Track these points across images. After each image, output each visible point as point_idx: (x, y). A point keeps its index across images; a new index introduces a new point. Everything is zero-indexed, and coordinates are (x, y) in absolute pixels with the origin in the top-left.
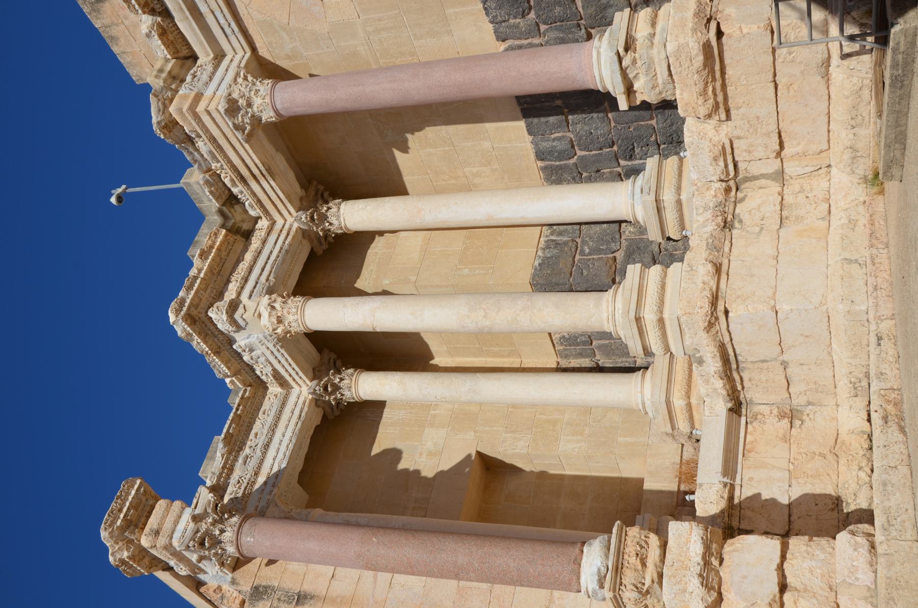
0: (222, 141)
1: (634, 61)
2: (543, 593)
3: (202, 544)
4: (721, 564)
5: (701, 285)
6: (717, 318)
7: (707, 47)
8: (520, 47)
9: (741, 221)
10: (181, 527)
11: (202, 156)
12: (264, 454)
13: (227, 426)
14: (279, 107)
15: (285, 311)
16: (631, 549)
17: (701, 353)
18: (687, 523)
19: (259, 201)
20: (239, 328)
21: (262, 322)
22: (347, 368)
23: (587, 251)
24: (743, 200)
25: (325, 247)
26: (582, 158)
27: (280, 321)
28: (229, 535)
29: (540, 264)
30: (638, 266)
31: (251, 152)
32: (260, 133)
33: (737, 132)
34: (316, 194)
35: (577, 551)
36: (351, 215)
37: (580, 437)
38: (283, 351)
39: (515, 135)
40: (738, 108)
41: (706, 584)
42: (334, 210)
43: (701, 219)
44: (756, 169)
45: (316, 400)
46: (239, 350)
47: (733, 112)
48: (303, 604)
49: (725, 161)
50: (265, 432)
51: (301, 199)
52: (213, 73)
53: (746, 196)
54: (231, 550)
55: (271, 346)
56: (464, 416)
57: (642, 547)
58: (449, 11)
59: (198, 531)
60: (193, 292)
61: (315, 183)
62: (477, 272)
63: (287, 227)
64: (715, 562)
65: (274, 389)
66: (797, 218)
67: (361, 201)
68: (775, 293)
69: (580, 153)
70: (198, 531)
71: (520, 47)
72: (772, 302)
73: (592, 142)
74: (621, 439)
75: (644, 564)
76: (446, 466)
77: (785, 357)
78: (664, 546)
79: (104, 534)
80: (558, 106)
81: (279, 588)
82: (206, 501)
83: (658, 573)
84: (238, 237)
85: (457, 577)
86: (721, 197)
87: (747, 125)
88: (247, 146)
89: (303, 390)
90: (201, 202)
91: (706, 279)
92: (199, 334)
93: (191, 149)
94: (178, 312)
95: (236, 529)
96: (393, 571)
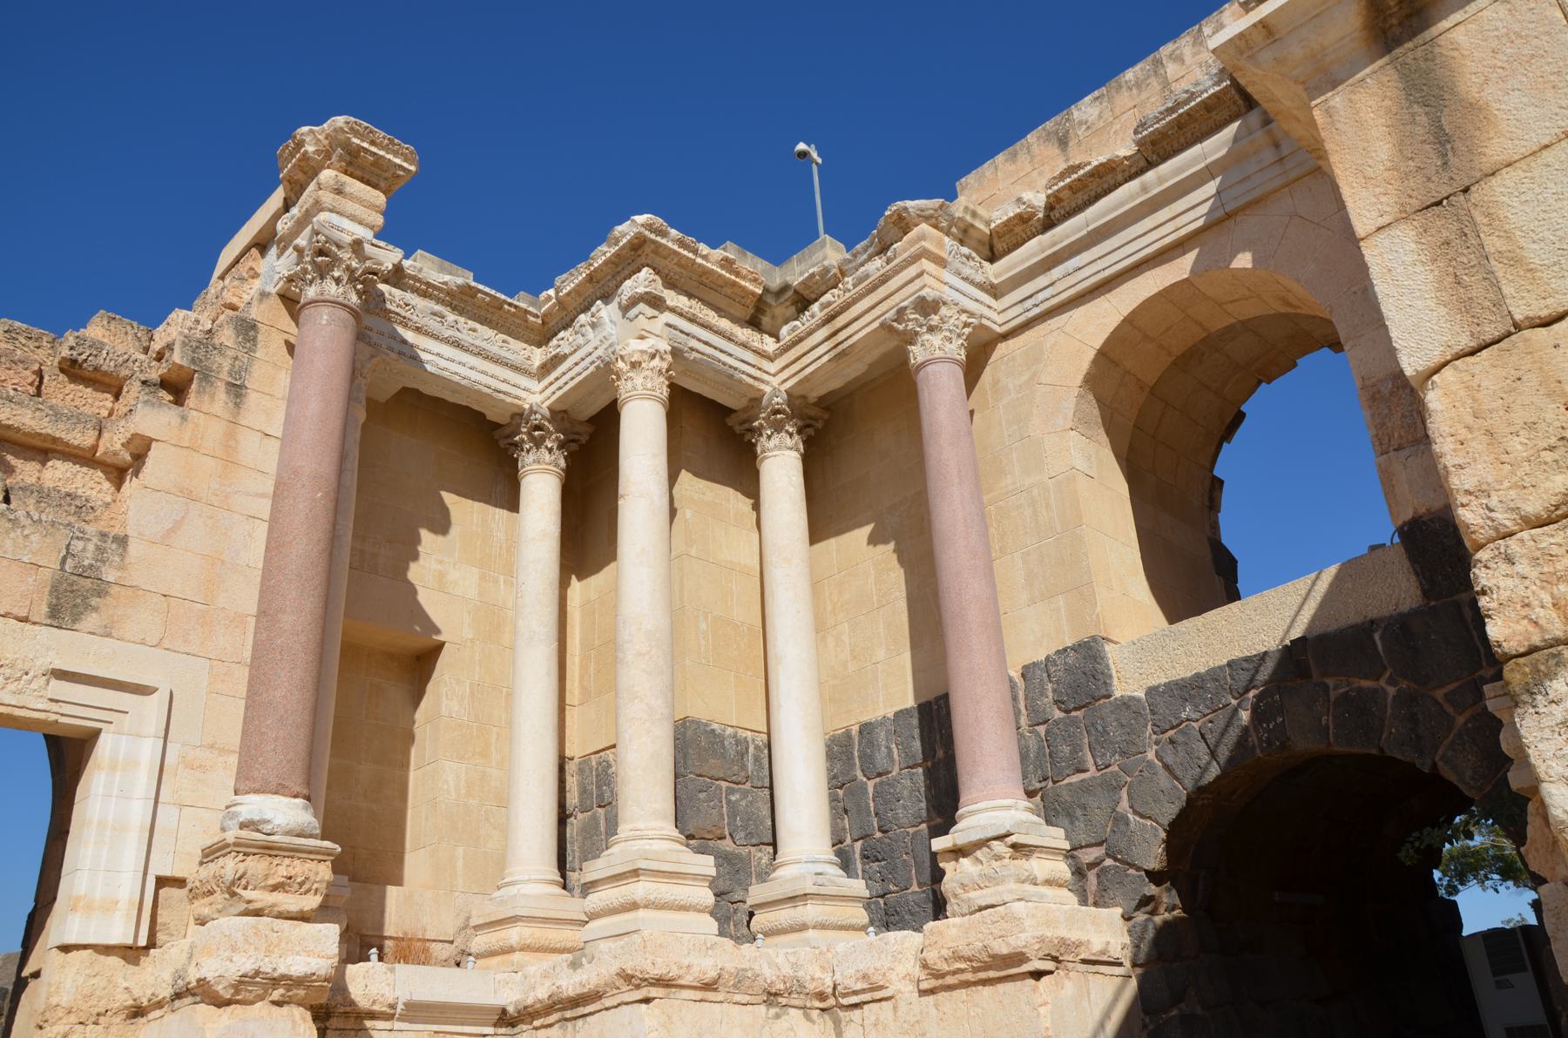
0: (882, 291)
1: (998, 858)
2: (235, 740)
3: (321, 252)
4: (274, 1003)
5: (686, 962)
6: (638, 987)
7: (1020, 958)
8: (1015, 699)
9: (777, 1016)
10: (346, 224)
11: (862, 265)
12: (446, 341)
13: (487, 290)
14: (930, 369)
15: (648, 373)
16: (299, 868)
18: (336, 951)
19: (801, 340)
20: (624, 309)
21: (634, 341)
22: (566, 458)
24: (808, 1018)
25: (738, 429)
26: (864, 788)
27: (635, 365)
28: (331, 289)
30: (713, 872)
31: (868, 330)
32: (893, 343)
33: (903, 1007)
35: (297, 789)
36: (782, 466)
38: (592, 368)
39: (894, 693)
40: (936, 1006)
41: (242, 982)
42: (789, 442)
43: (780, 960)
45: (521, 415)
46: (593, 309)
47: (931, 999)
48: (228, 393)
49: (863, 991)
50: (477, 342)
51: (804, 397)
52: (972, 283)
53: (813, 1022)
54: (311, 292)
55: (600, 352)
56: (495, 624)
57: (301, 884)
58: (1061, 601)
59: (339, 247)
60: (675, 247)
61: (826, 416)
63: (766, 377)
64: (277, 995)
65: (538, 356)
67: (801, 480)
69: (871, 785)
70: (339, 247)
71: (1015, 699)
73: (886, 802)
74: (460, 850)
76: (423, 597)
78: (303, 917)
79: (340, 121)
81: (252, 359)
83: (262, 910)
84: (751, 311)
85: (262, 613)
86: (811, 987)
88: (876, 325)
89: (536, 396)
90: (800, 262)
91: (695, 969)
92: (617, 255)
93: (871, 250)
94: (649, 227)
95: (341, 299)
96: (273, 521)
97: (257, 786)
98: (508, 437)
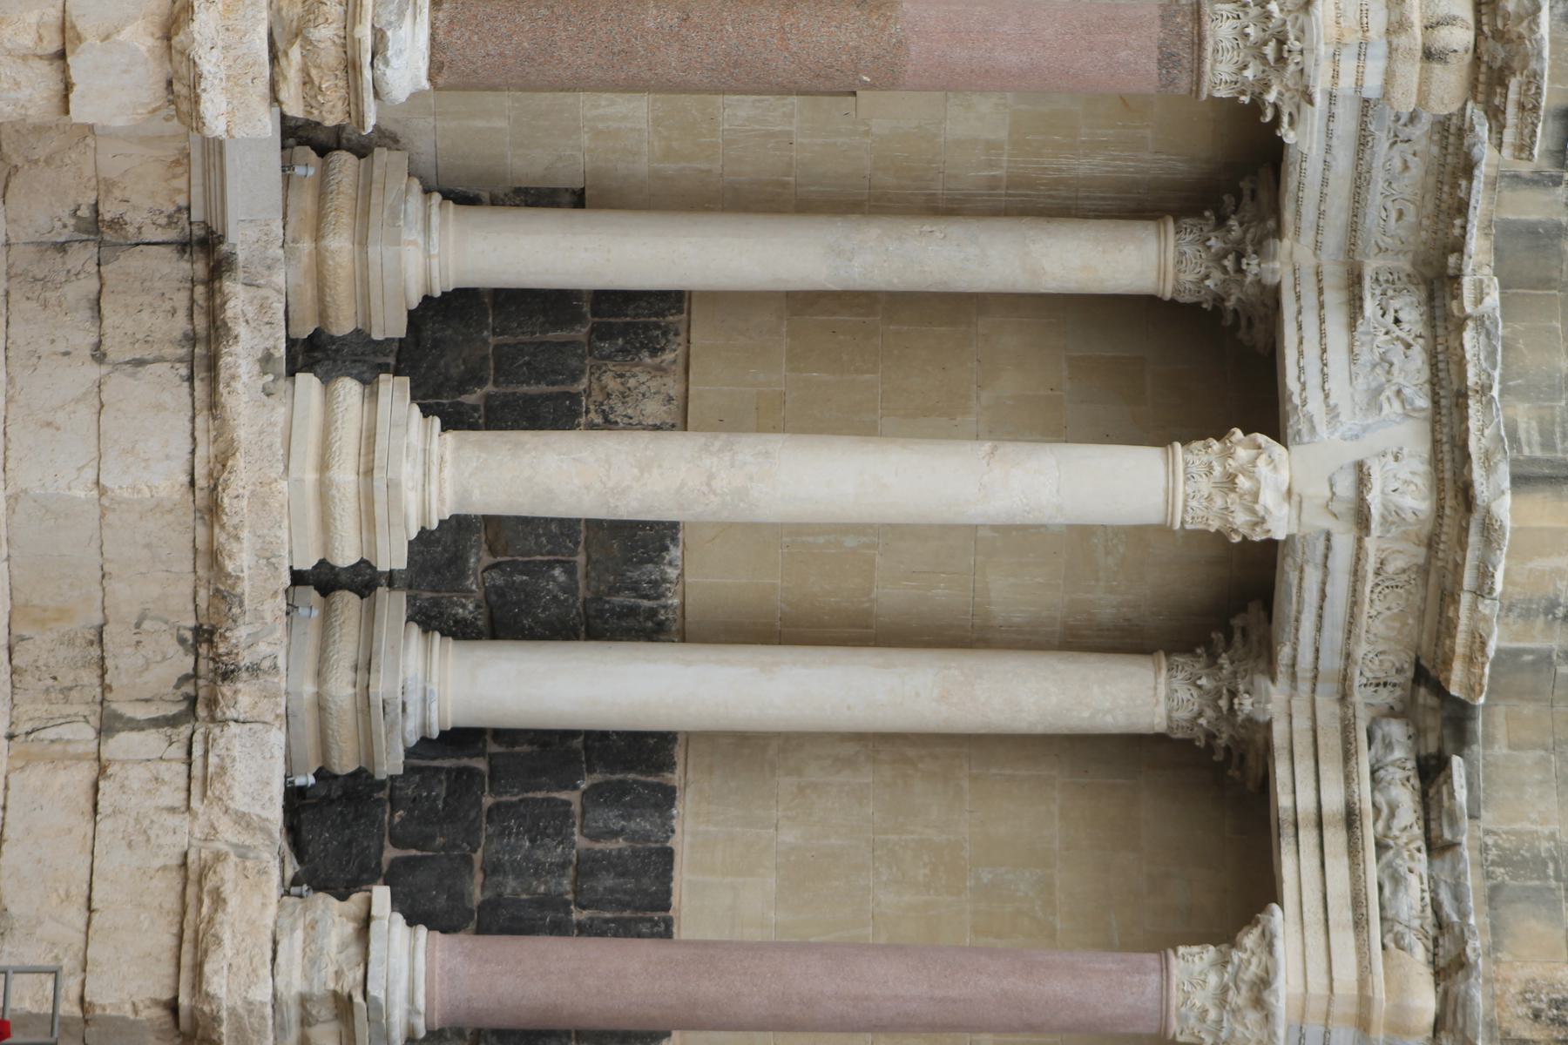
0: (1341, 913)
1: (339, 974)
9: (182, 641)
14: (1154, 979)
15: (1219, 502)
17: (260, 383)
23: (557, 572)
24: (185, 679)
25: (1237, 622)
26: (565, 788)
27: (1230, 481)
29: (667, 549)
34: (1242, 758)
37: (601, 126)
40: (164, 868)
43: (263, 648)
44: (152, 741)
49: (206, 766)
50: (1379, 177)
53: (177, 687)
55: (1315, 406)
62: (821, 540)
63: (1304, 687)
66: (71, 643)
68: (102, 516)
72: (105, 501)
74: (501, 123)
75: (307, 81)
77: (95, 372)
80: (584, 908)
82: (1300, 128)
87: (152, 833)
91: (235, 546)
97: (441, 37)
98: (1254, 196)
